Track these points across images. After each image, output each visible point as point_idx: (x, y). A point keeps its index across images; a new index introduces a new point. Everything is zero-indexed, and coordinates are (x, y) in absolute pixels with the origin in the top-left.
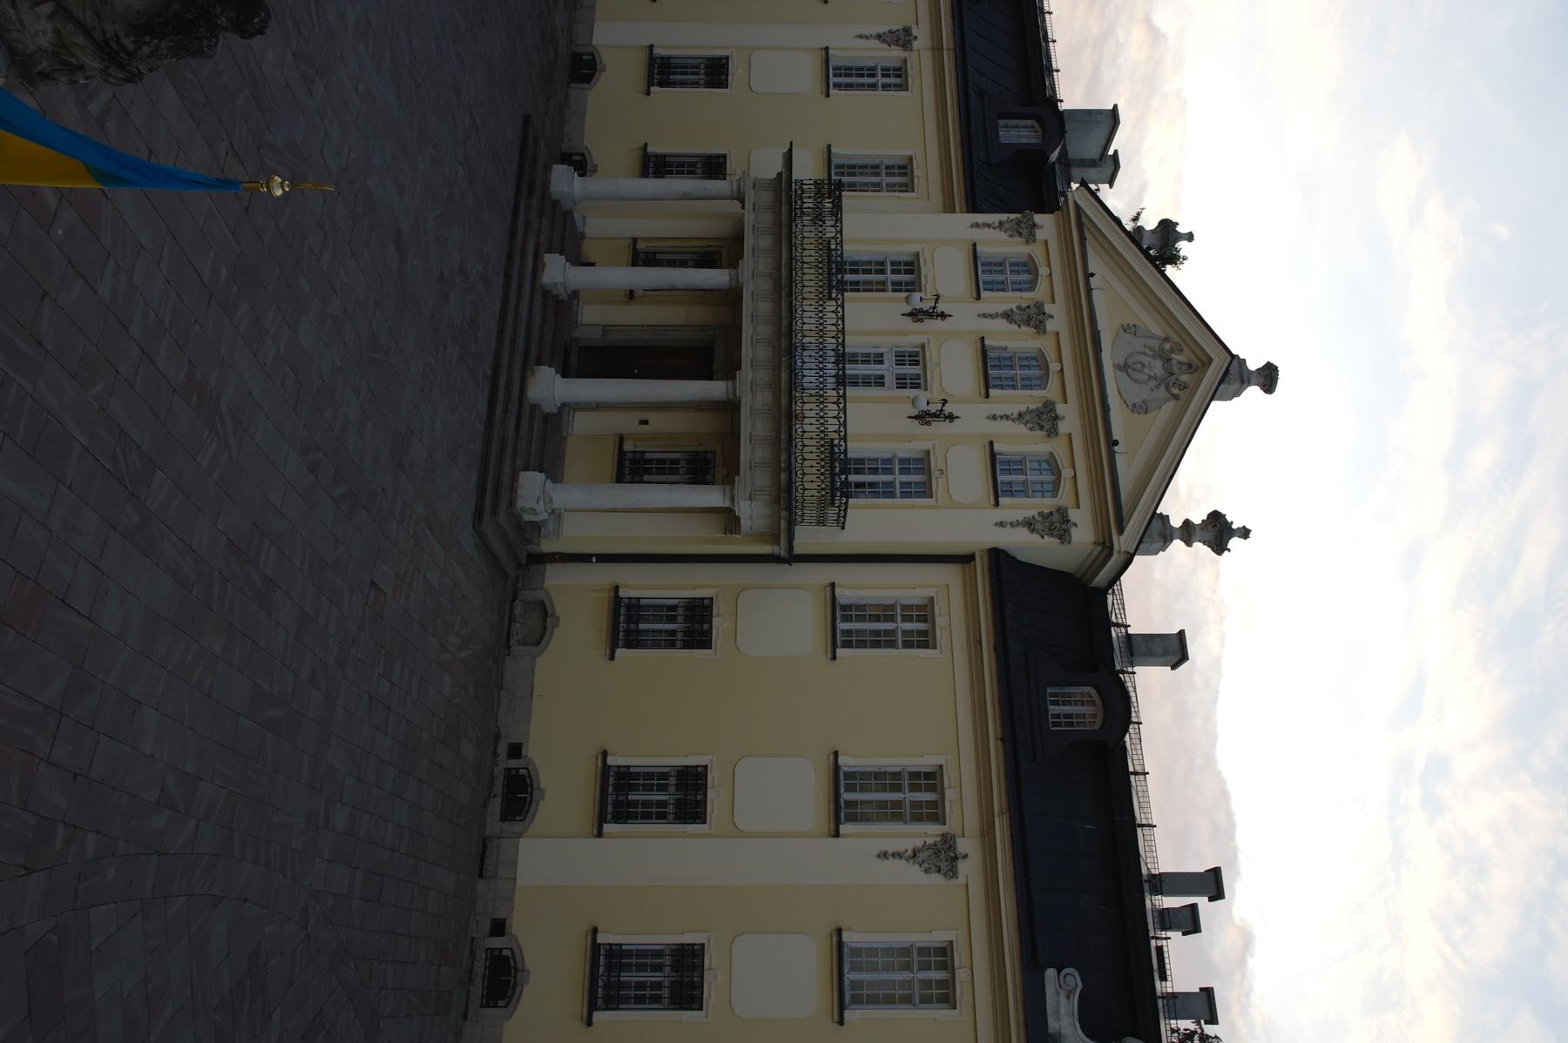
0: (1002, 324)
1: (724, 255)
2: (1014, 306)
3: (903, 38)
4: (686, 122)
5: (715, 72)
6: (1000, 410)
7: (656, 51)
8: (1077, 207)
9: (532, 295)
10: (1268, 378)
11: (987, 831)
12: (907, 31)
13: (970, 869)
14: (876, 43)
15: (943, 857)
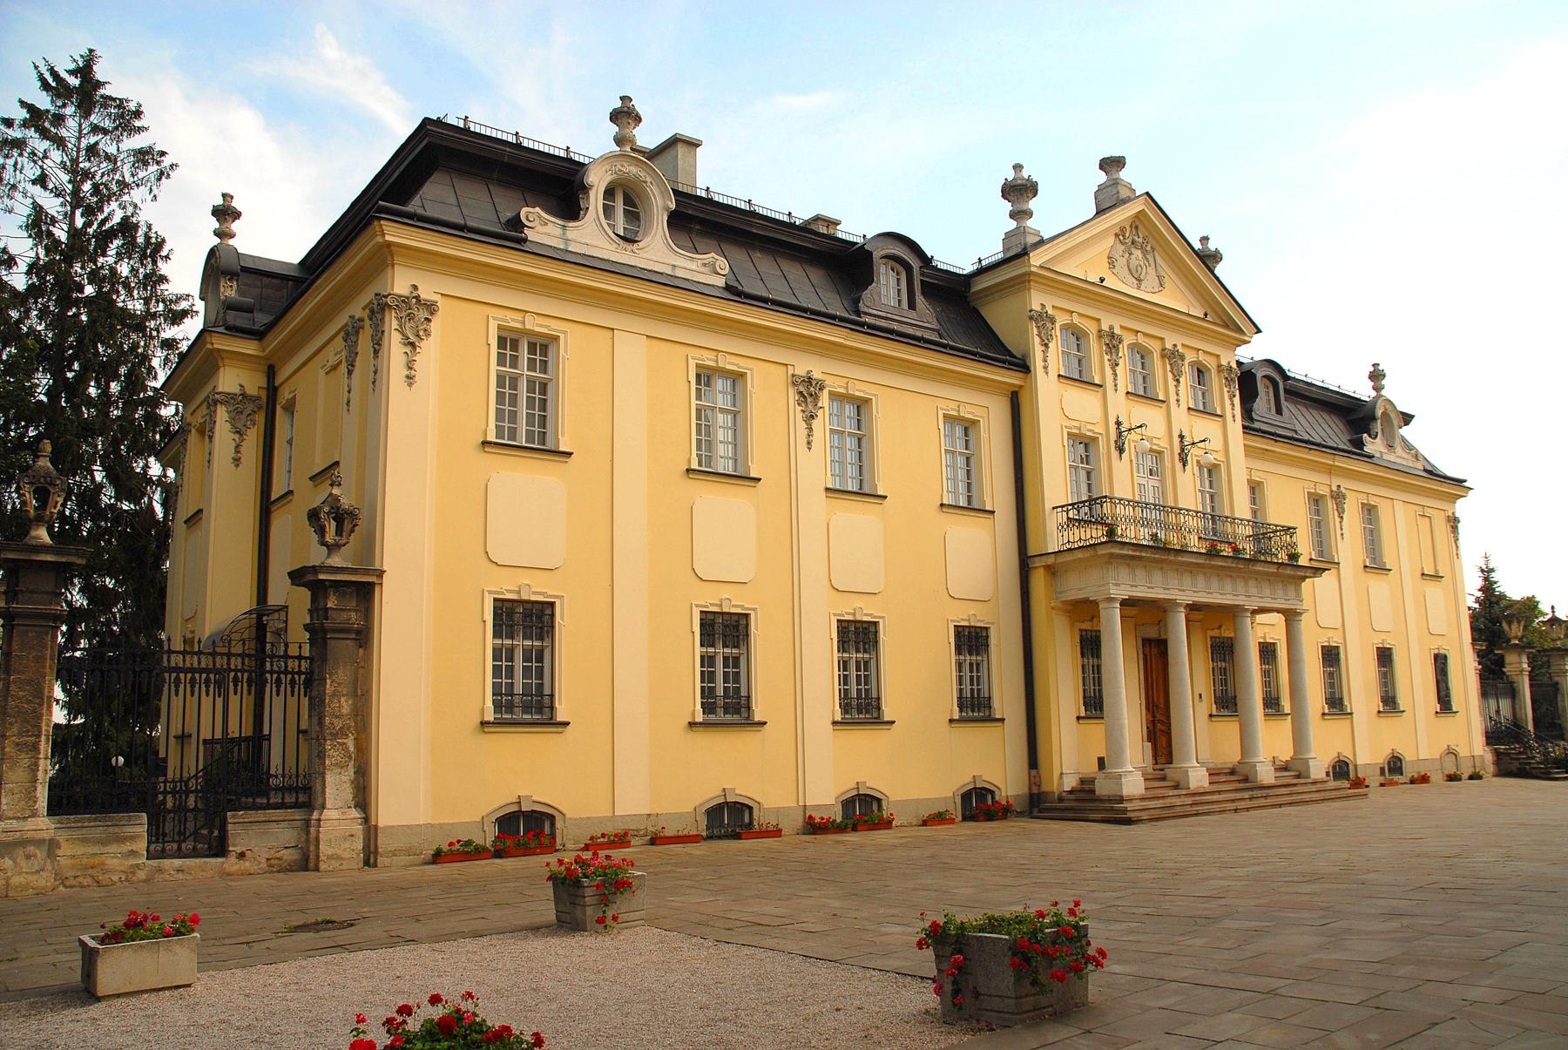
0: (1119, 370)
1: (1086, 626)
2: (1106, 357)
3: (807, 390)
4: (916, 672)
5: (858, 637)
6: (1173, 398)
7: (838, 718)
8: (1041, 267)
9: (1219, 792)
10: (1111, 164)
11: (1330, 470)
12: (795, 381)
13: (1346, 484)
14: (816, 423)
15: (1338, 497)
